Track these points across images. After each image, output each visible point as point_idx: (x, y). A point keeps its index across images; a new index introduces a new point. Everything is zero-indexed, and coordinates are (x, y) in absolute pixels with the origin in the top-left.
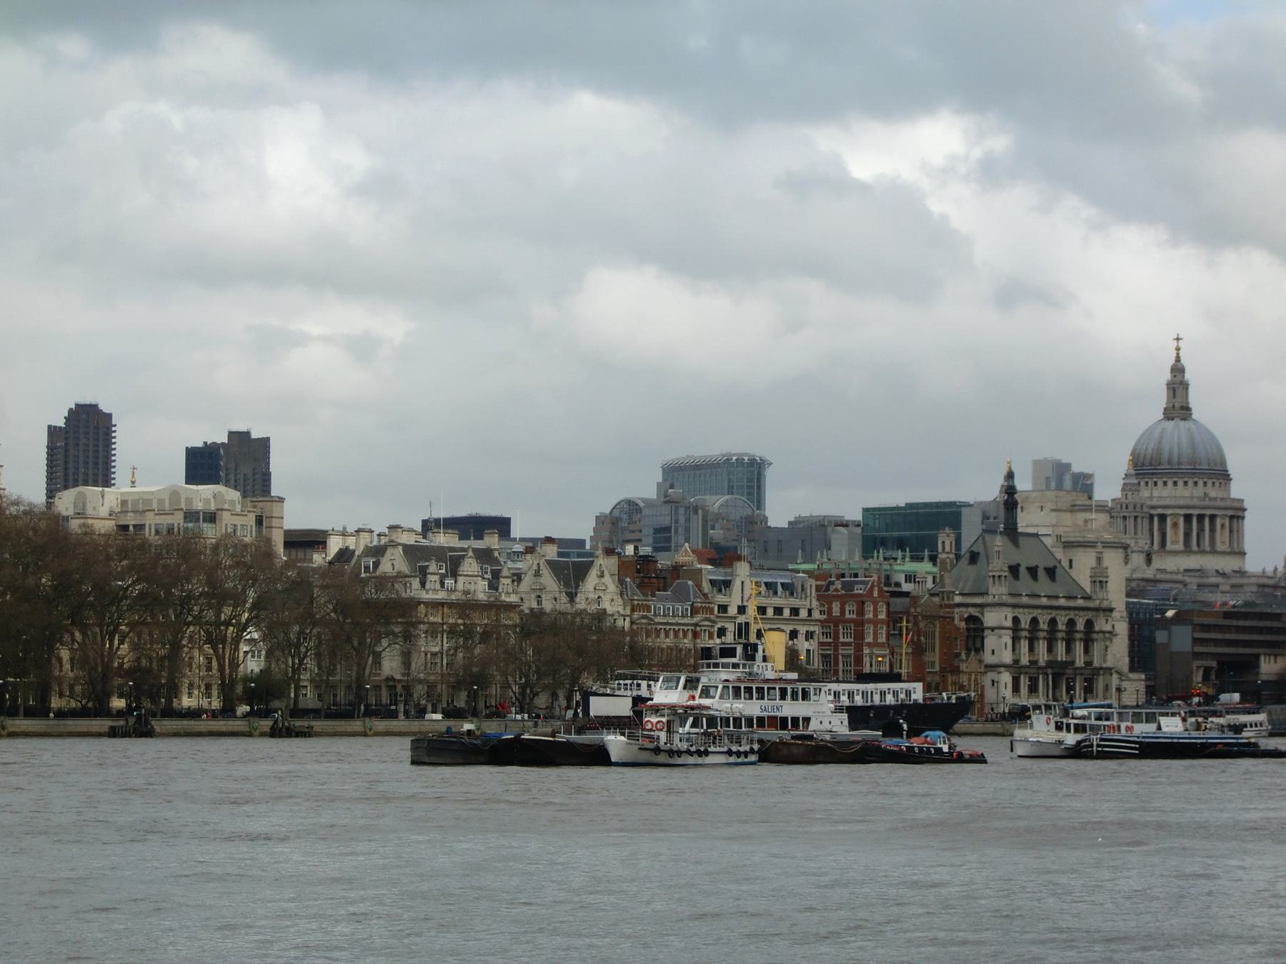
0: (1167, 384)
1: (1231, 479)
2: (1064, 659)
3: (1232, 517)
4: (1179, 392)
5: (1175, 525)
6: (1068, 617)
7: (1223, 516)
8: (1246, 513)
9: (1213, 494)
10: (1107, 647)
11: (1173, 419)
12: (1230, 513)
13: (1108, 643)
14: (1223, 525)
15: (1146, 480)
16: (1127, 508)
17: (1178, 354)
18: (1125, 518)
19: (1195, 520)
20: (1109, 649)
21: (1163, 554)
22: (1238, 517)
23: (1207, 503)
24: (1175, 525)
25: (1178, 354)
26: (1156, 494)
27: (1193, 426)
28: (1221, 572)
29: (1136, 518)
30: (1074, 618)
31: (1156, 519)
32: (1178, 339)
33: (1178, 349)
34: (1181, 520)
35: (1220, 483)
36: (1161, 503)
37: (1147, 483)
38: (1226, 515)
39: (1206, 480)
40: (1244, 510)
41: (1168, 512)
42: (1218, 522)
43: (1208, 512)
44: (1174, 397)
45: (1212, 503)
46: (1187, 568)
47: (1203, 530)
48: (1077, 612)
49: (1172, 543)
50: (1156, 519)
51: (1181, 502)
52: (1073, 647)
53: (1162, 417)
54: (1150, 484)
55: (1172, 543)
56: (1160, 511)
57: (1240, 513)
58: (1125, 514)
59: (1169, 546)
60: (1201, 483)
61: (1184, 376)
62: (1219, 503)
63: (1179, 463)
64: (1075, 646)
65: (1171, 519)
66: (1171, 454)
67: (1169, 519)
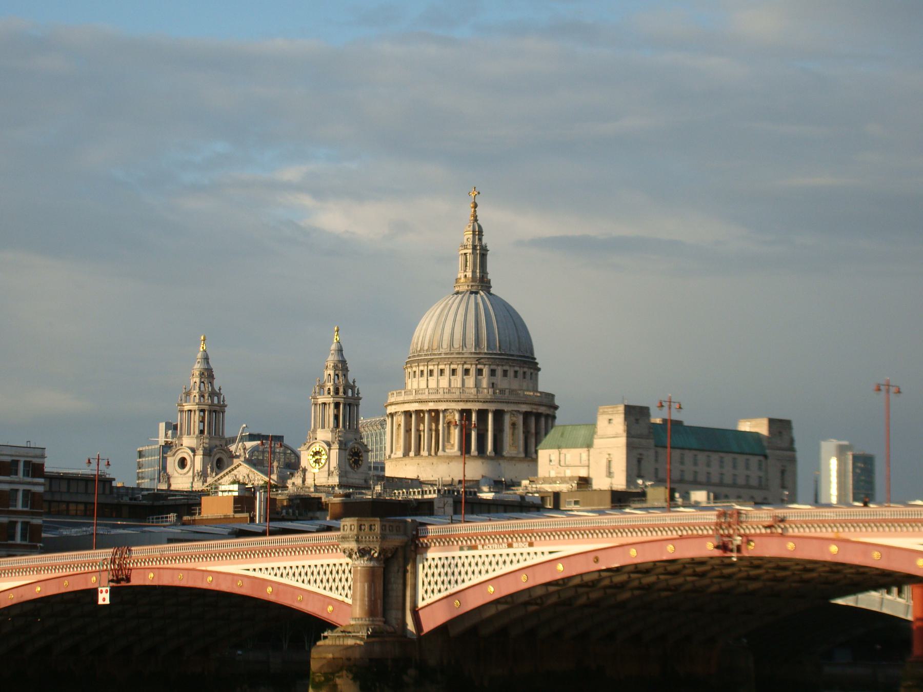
1: (539, 369)
3: (527, 415)
7: (512, 413)
8: (558, 413)
12: (525, 408)
14: (514, 425)
16: (329, 393)
17: (475, 211)
21: (435, 460)
22: (538, 416)
25: (475, 211)
26: (433, 383)
29: (337, 405)
33: (475, 206)
35: (516, 372)
37: (422, 372)
38: (518, 411)
39: (493, 367)
40: (556, 408)
41: (441, 406)
42: (507, 420)
47: (487, 430)
54: (425, 373)
56: (431, 406)
57: (542, 410)
61: (480, 240)
65: (444, 417)
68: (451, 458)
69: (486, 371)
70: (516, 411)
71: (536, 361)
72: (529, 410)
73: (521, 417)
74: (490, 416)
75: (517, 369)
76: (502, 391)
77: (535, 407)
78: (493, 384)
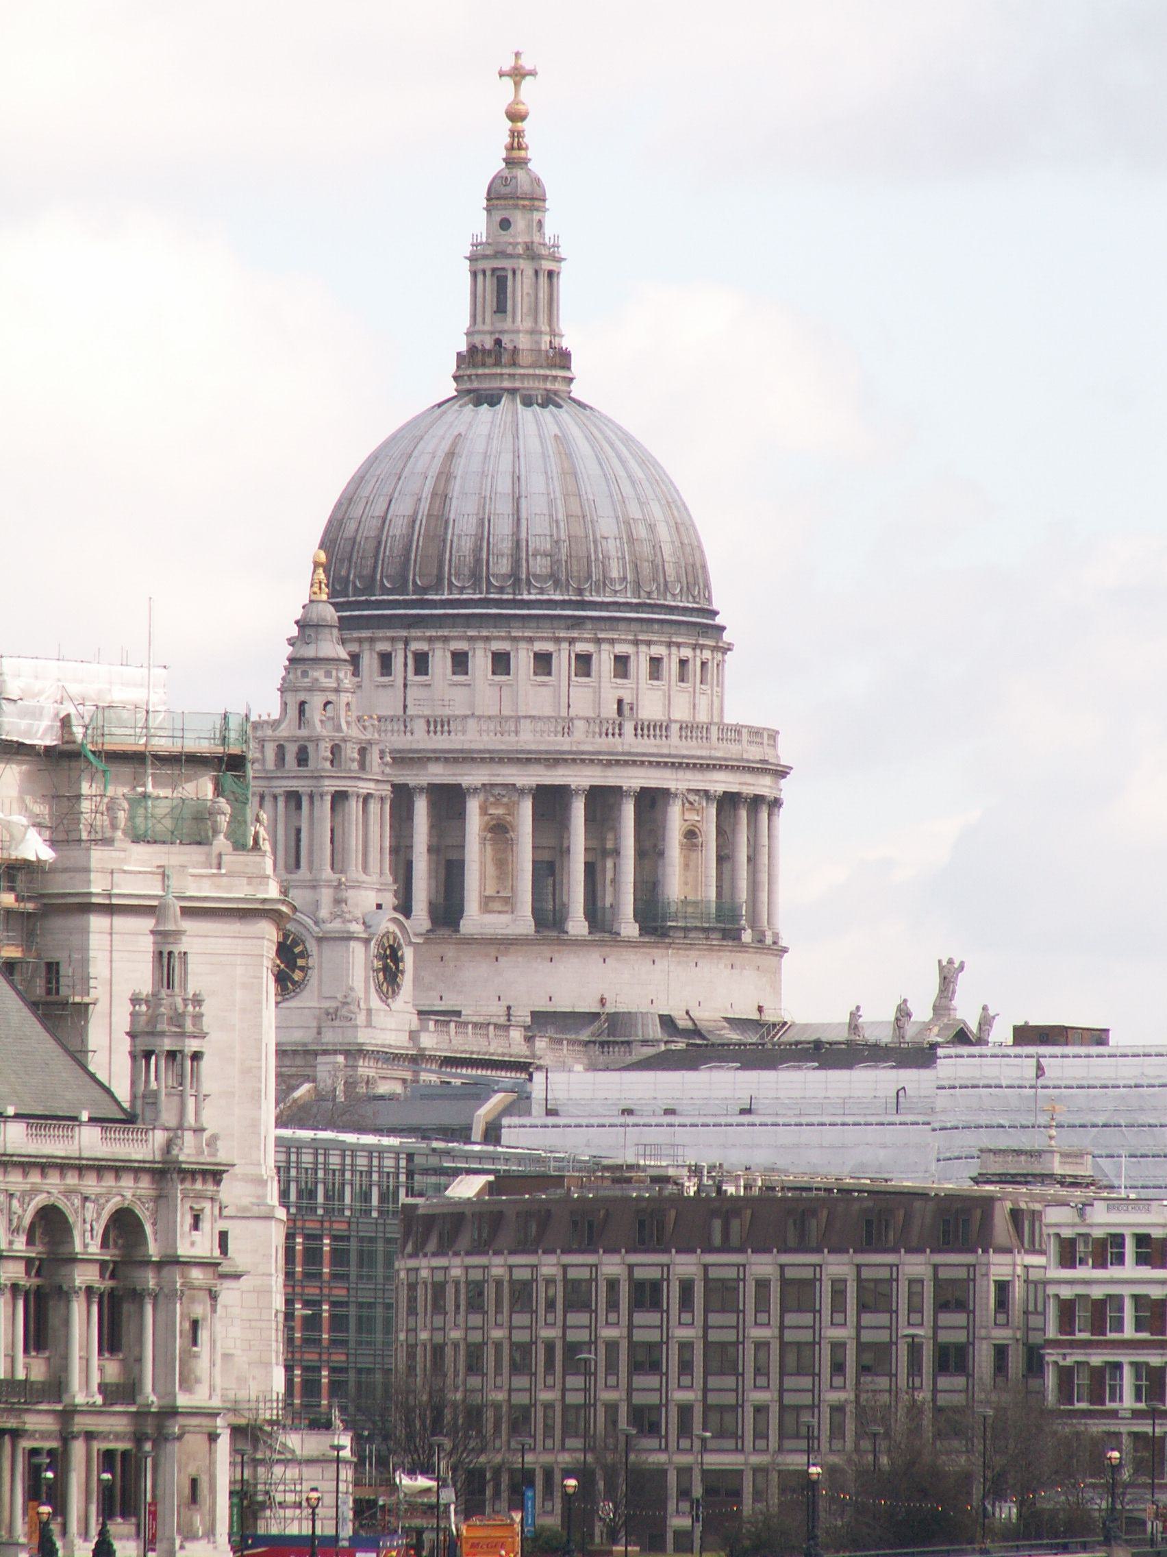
0: (473, 259)
1: (727, 649)
2: (21, 1375)
3: (728, 802)
4: (521, 289)
5: (500, 831)
6: (39, 1201)
8: (787, 789)
9: (651, 708)
10: (195, 1324)
11: (493, 401)
12: (722, 783)
13: (199, 1310)
15: (383, 646)
17: (516, 135)
18: (294, 798)
19: (578, 809)
20: (204, 1335)
21: (450, 952)
22: (756, 801)
23: (629, 742)
24: (500, 831)
25: (516, 135)
27: (575, 432)
28: (683, 1023)
30: (62, 1204)
31: (421, 807)
32: (518, 74)
34: (526, 808)
36: (441, 742)
39: (621, 649)
42: (676, 820)
43: (634, 779)
44: (501, 308)
45: (647, 745)
46: (543, 1006)
47: (616, 852)
48: (72, 1179)
49: (486, 904)
50: (421, 807)
51: (528, 739)
52: (54, 1320)
53: (450, 389)
55: (486, 904)
56: (438, 774)
57: (762, 786)
58: (294, 785)
59: (474, 919)
60: (604, 662)
62: (676, 745)
63: (515, 578)
64: (67, 1322)
65: (484, 810)
66: (482, 537)
67: (473, 806)
68: (503, 944)
69: (604, 662)
70: (697, 792)
71: (718, 620)
72: (734, 789)
73: (713, 811)
74: (628, 811)
75: (686, 653)
76: (659, 728)
77: (748, 778)
78: (620, 702)
